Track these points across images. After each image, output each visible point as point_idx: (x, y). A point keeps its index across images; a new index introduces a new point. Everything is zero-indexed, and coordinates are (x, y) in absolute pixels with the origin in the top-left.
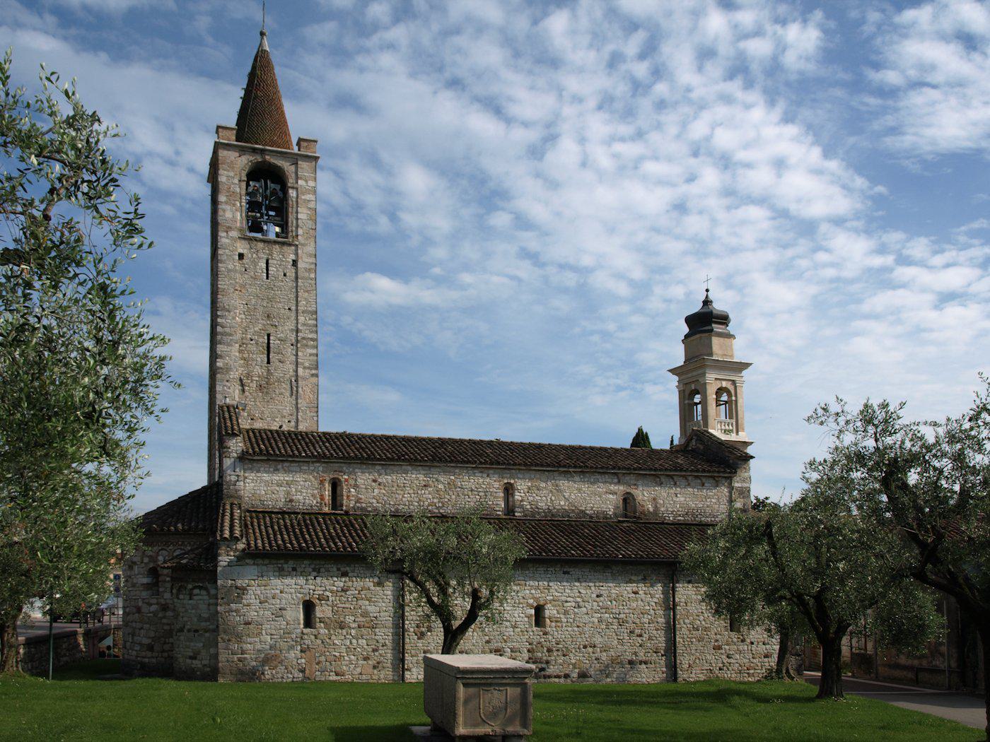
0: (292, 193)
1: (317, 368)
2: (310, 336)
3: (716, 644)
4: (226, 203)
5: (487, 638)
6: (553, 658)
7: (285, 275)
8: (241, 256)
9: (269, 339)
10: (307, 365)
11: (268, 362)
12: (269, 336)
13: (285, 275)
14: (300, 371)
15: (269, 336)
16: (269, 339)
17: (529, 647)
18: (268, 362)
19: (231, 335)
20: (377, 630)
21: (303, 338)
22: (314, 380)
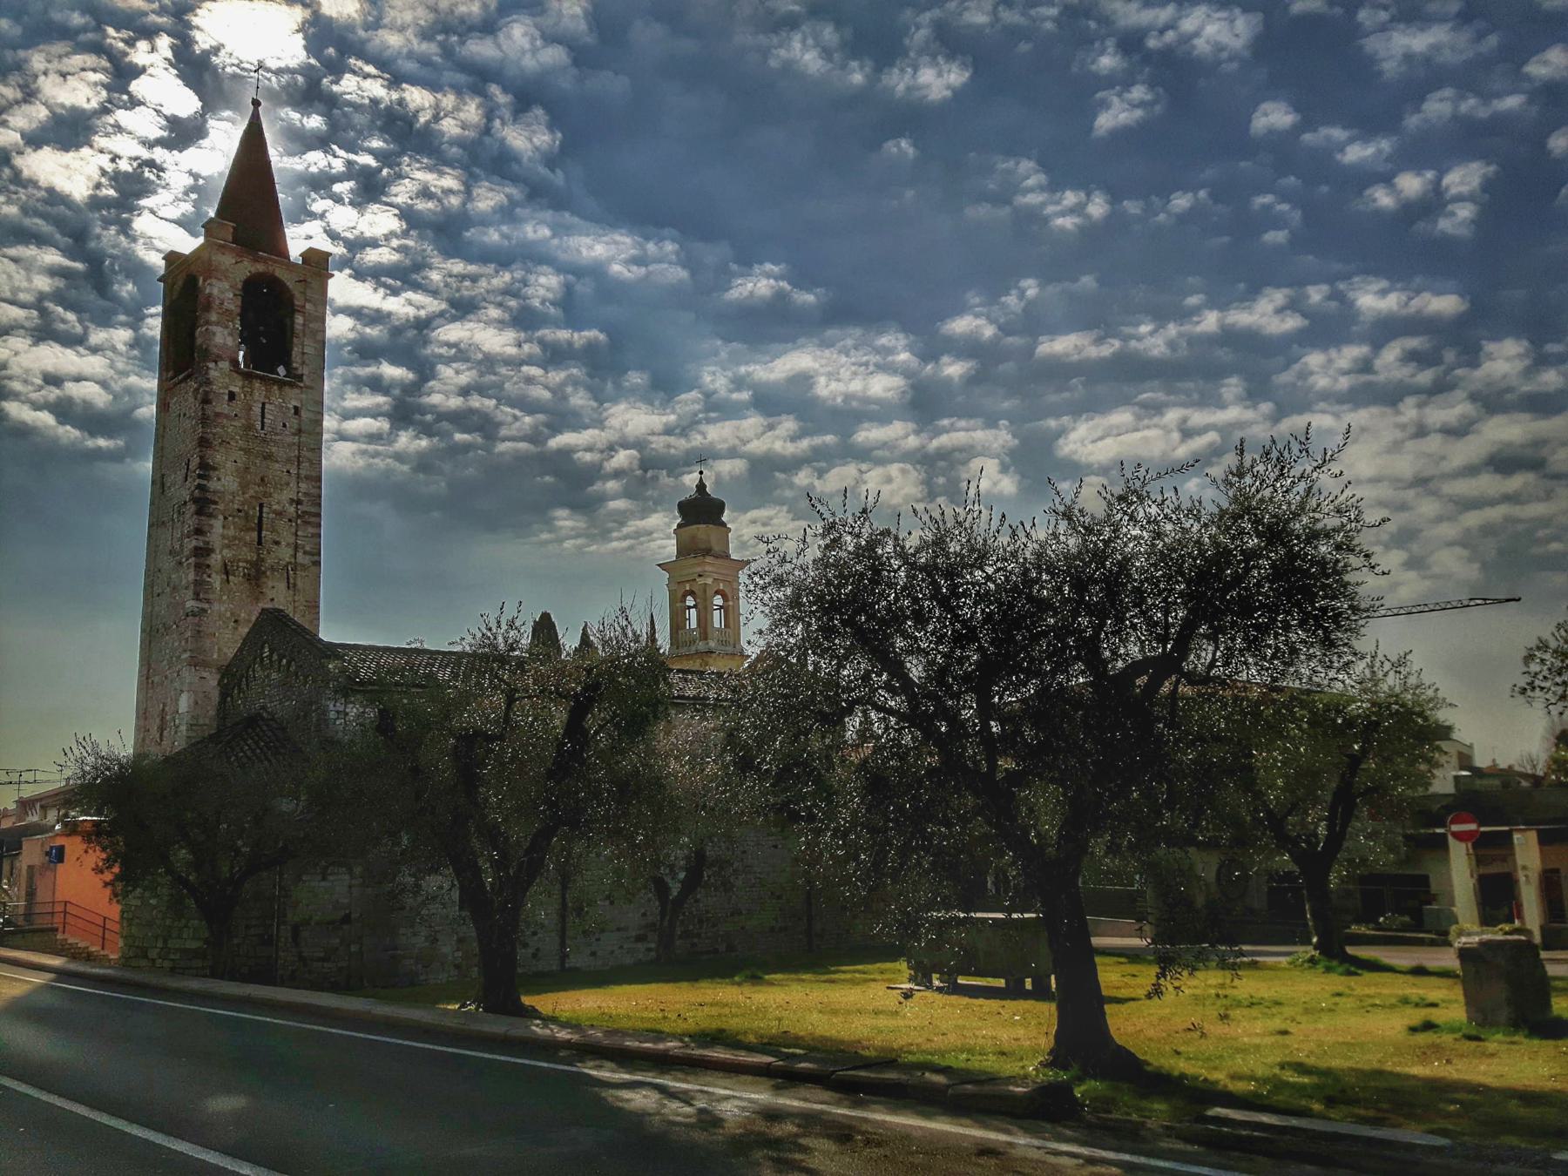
4: (217, 324)
8: (232, 396)
9: (261, 512)
12: (261, 506)
14: (300, 555)
15: (261, 506)
16: (261, 512)
19: (215, 503)
21: (305, 512)
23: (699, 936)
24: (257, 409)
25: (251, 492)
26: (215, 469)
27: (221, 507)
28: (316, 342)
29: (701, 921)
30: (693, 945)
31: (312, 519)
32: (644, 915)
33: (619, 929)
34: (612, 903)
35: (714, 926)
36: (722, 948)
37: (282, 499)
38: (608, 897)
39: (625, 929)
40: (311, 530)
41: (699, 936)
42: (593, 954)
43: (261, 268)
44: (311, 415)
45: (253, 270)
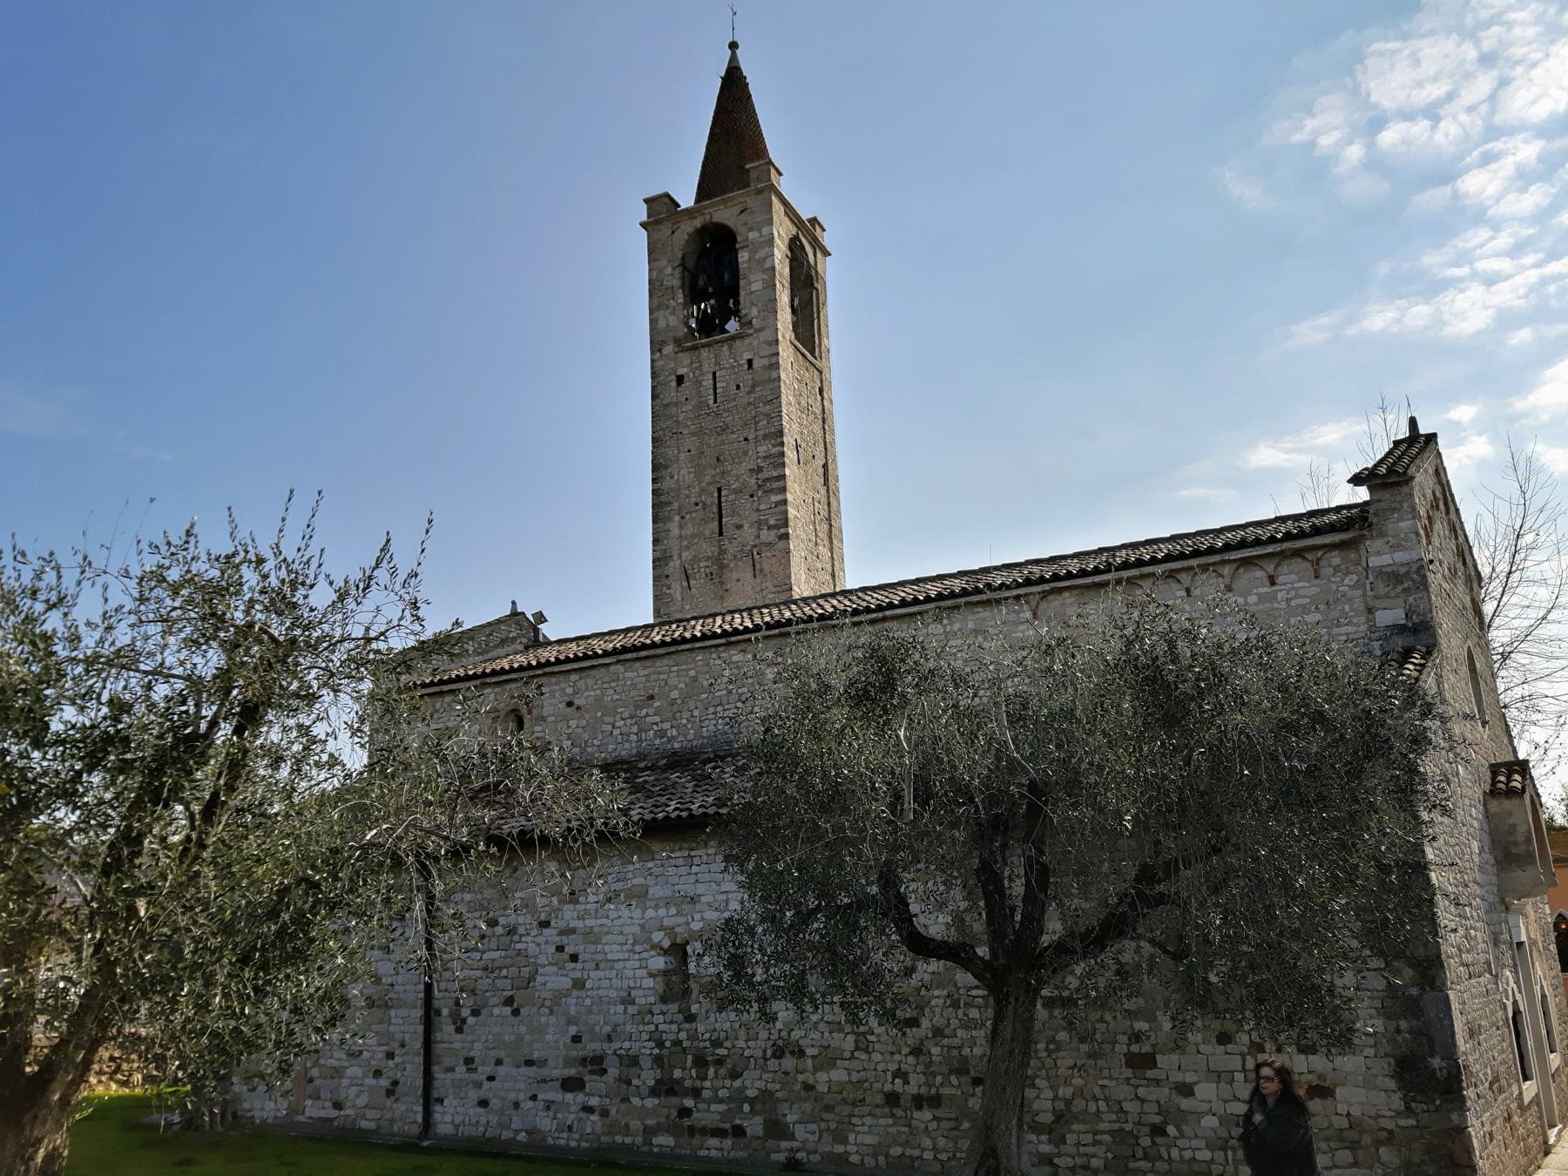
0: (743, 256)
1: (786, 525)
2: (775, 474)
3: (1135, 1048)
5: (573, 1030)
6: (707, 1084)
7: (738, 387)
8: (680, 379)
9: (720, 497)
10: (772, 522)
11: (721, 534)
12: (719, 490)
13: (738, 387)
15: (719, 490)
16: (720, 497)
17: (656, 1051)
18: (721, 534)
20: (393, 1012)
21: (767, 480)
22: (781, 544)
23: (696, 1093)
24: (708, 383)
25: (708, 479)
26: (666, 467)
27: (675, 506)
28: (765, 271)
29: (701, 1062)
30: (685, 1112)
31: (776, 485)
32: (576, 1039)
33: (529, 1063)
34: (516, 1012)
35: (735, 1075)
36: (755, 1126)
37: (740, 473)
38: (509, 1001)
39: (542, 1063)
40: (775, 498)
41: (696, 1093)
42: (483, 1103)
43: (698, 223)
44: (766, 362)
45: (690, 230)
